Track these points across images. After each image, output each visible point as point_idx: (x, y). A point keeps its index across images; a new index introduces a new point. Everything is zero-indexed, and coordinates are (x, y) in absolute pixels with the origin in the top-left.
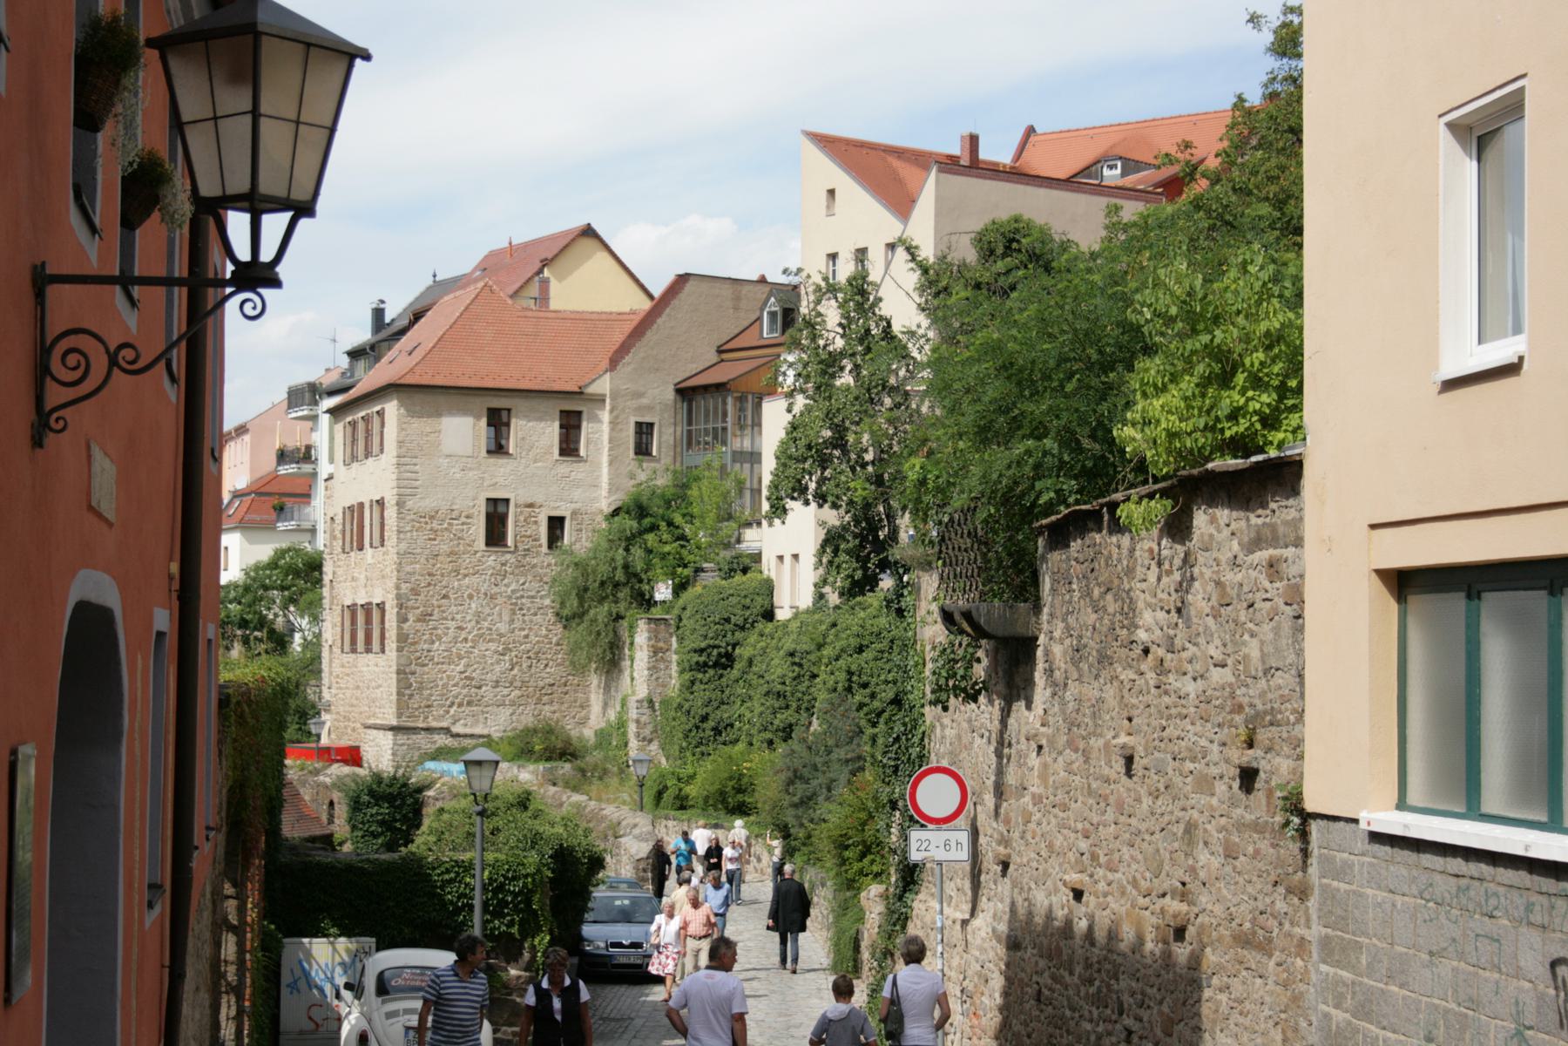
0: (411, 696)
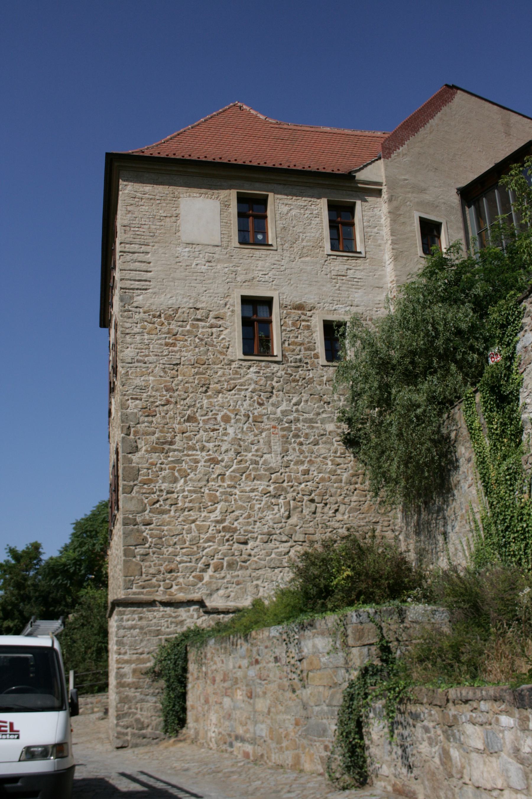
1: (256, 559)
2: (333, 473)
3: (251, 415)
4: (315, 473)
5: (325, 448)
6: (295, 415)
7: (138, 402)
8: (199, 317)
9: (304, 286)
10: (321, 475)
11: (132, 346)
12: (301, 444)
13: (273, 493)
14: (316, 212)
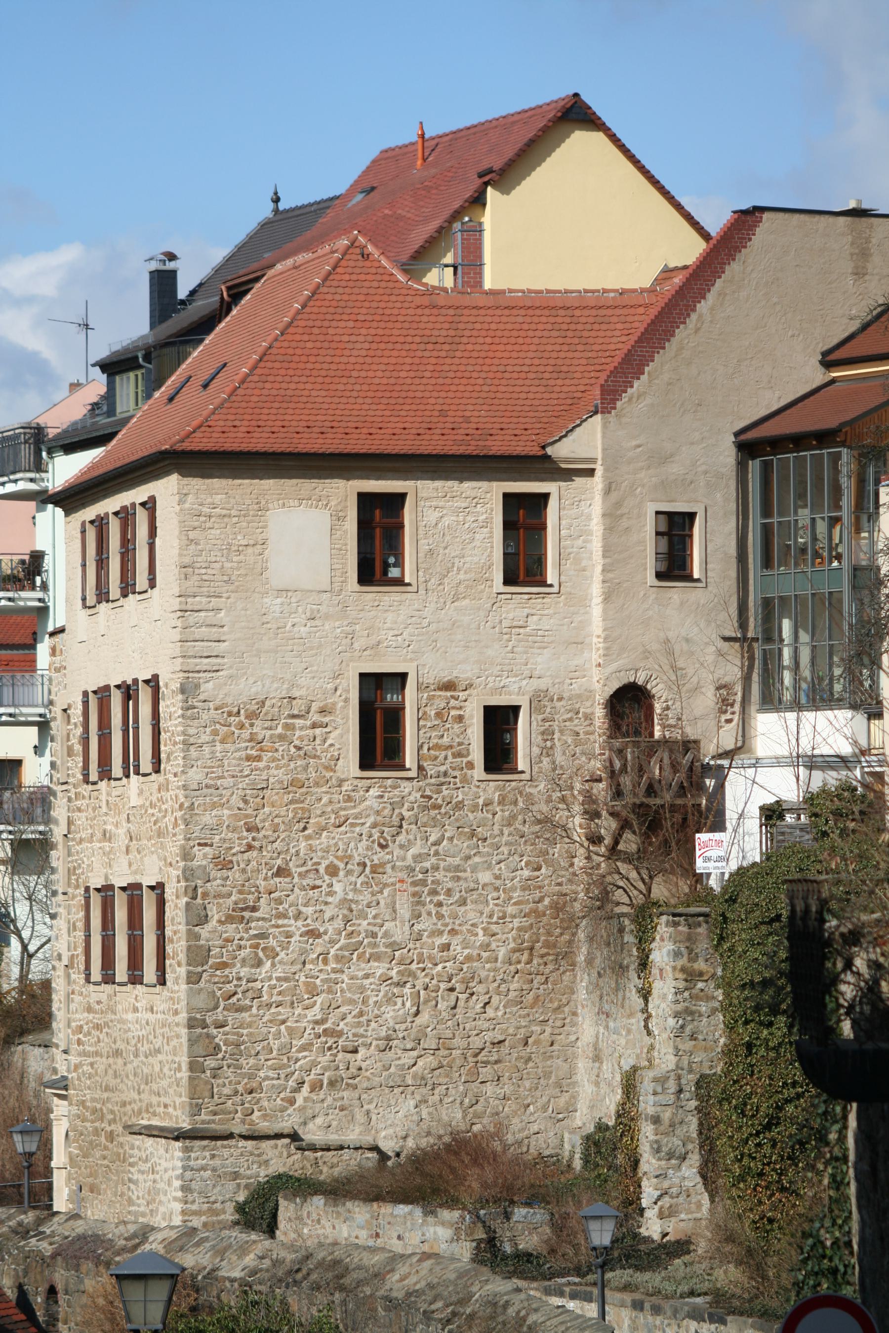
0: (216, 1072)
1: (368, 1074)
2: (486, 947)
3: (369, 864)
4: (459, 948)
5: (475, 910)
6: (433, 860)
7: (207, 848)
8: (296, 712)
9: (457, 650)
10: (466, 952)
11: (199, 763)
12: (440, 904)
13: (395, 980)
14: (484, 517)
